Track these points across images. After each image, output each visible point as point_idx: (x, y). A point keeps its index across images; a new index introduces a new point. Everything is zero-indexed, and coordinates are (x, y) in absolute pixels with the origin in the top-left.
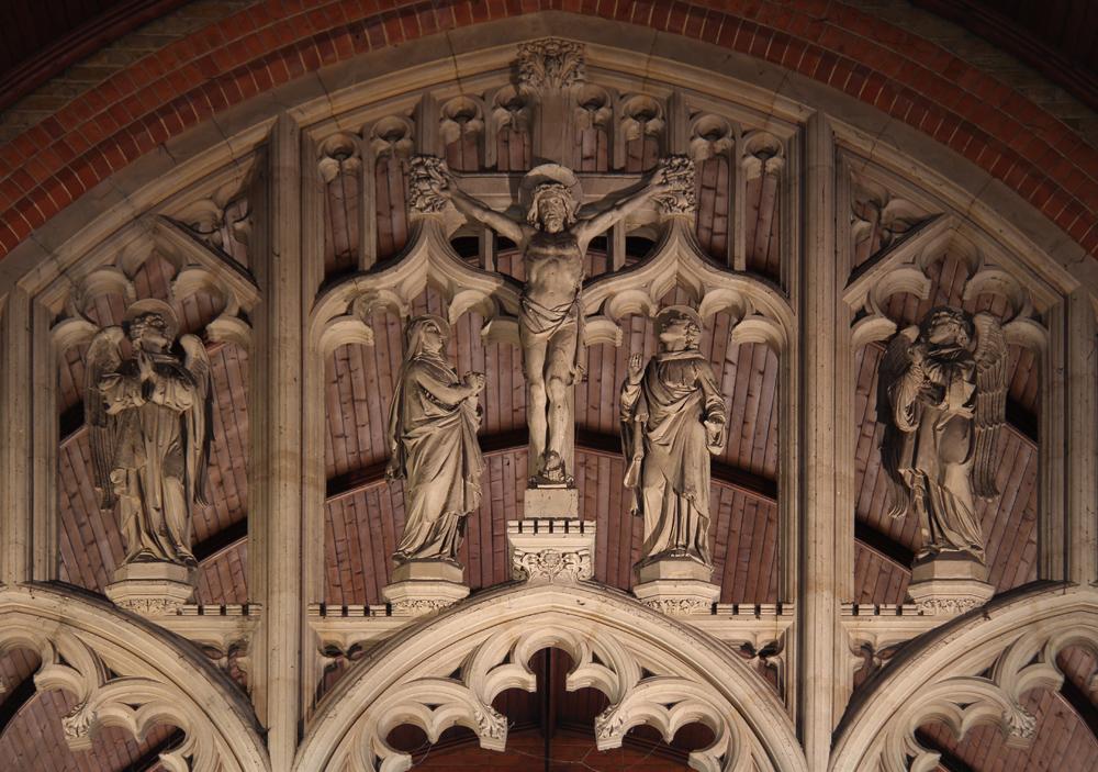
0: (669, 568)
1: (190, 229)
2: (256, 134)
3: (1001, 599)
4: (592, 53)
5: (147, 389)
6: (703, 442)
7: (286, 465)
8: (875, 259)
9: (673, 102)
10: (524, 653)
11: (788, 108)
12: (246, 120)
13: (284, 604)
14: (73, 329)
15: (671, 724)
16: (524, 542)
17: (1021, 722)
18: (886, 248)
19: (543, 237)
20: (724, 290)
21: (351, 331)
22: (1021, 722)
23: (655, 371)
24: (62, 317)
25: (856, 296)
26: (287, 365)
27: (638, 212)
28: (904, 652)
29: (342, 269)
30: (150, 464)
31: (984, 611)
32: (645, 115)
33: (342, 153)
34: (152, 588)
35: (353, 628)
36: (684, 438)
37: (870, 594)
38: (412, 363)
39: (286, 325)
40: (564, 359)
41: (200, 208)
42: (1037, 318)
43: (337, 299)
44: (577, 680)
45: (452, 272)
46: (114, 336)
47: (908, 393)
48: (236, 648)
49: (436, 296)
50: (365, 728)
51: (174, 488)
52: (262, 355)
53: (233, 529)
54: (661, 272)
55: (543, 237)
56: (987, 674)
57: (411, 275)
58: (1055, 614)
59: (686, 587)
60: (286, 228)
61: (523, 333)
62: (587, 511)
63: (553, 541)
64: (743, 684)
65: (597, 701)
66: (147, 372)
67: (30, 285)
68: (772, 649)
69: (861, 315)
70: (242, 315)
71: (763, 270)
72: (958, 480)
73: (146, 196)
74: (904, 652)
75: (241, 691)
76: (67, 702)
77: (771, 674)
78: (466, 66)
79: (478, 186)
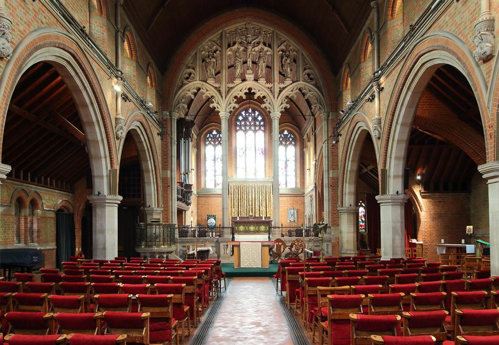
0: (261, 79)
1: (214, 42)
2: (221, 31)
3: (293, 82)
4: (253, 23)
5: (211, 59)
6: (264, 65)
7: (224, 68)
8: (280, 45)
9: (261, 28)
10: (247, 89)
11: (271, 29)
12: (220, 30)
13: (224, 83)
14: (203, 52)
15: (261, 96)
16: (247, 76)
17: (295, 96)
18: (281, 44)
19: (248, 43)
20: (266, 48)
21: (230, 53)
22: (295, 96)
23: (259, 57)
24: (202, 51)
25: (278, 49)
26: (224, 57)
27: (257, 40)
28: (284, 88)
29: (229, 46)
30: (211, 67)
31: (291, 84)
32: (258, 29)
33: (229, 33)
34: (211, 81)
35: (231, 85)
36: (262, 64)
37: (282, 82)
38: (236, 56)
39: (224, 53)
40: (251, 56)
41: (215, 39)
42: (296, 52)
43: (229, 49)
44: (252, 91)
45: (240, 47)
46: (207, 53)
47: (284, 60)
48: (219, 87)
49: (238, 49)
50: (232, 97)
51: (213, 70)
52: (221, 55)
53: (219, 73)
54: (261, 45)
55: (248, 43)
56: (292, 91)
57: (236, 46)
58: (299, 84)
59: (262, 81)
60: (224, 42)
61: (246, 53)
62: (253, 73)
63: (250, 76)
64: (269, 92)
65: (254, 93)
66: (210, 57)
67: (199, 48)
68: (271, 88)
69: (279, 51)
70: (220, 51)
71: (270, 46)
72: (289, 69)
73: (210, 38)
74: (284, 88)
75: (219, 91)
76: (203, 93)
77: (271, 90)
78: (241, 24)
79: (242, 37)
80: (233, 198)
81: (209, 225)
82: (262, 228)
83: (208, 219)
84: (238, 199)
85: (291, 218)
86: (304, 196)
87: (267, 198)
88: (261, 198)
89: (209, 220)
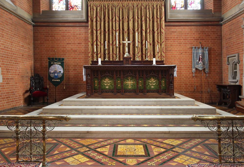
80: (95, 28)
81: (52, 75)
82: (152, 83)
83: (50, 65)
84: (105, 30)
85: (198, 63)
86: (221, 25)
87: (156, 29)
88: (144, 28)
89: (52, 67)
